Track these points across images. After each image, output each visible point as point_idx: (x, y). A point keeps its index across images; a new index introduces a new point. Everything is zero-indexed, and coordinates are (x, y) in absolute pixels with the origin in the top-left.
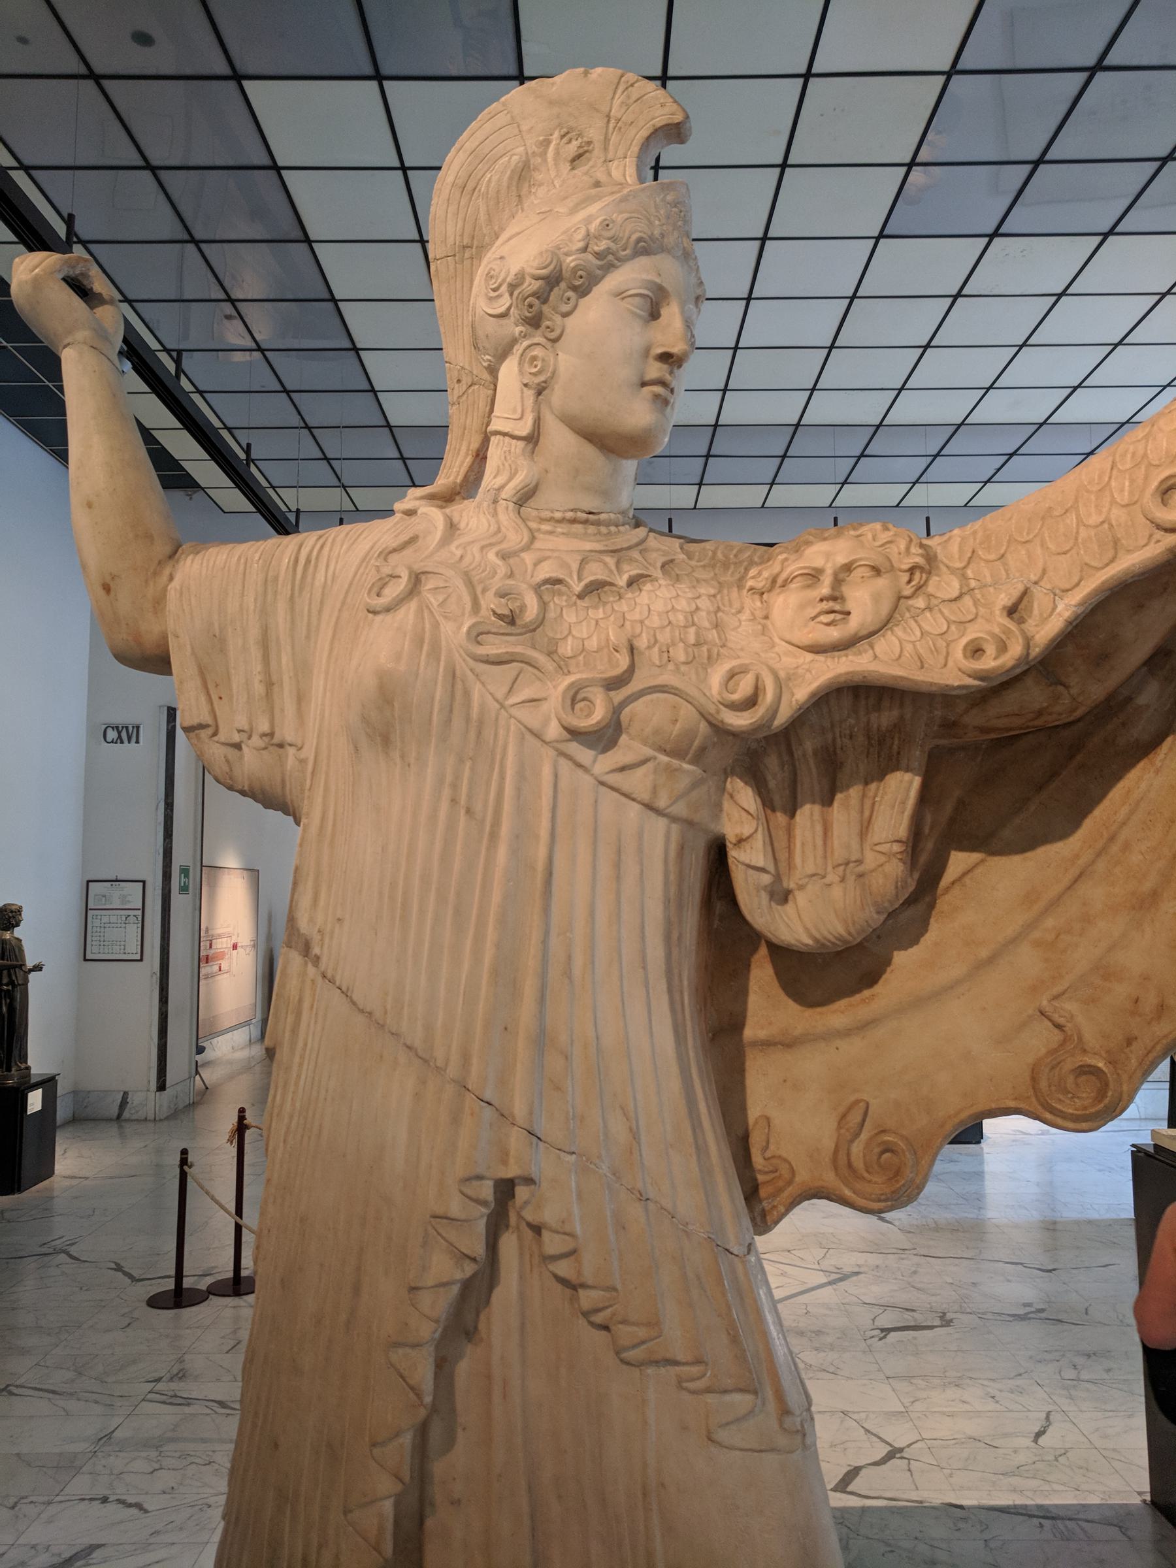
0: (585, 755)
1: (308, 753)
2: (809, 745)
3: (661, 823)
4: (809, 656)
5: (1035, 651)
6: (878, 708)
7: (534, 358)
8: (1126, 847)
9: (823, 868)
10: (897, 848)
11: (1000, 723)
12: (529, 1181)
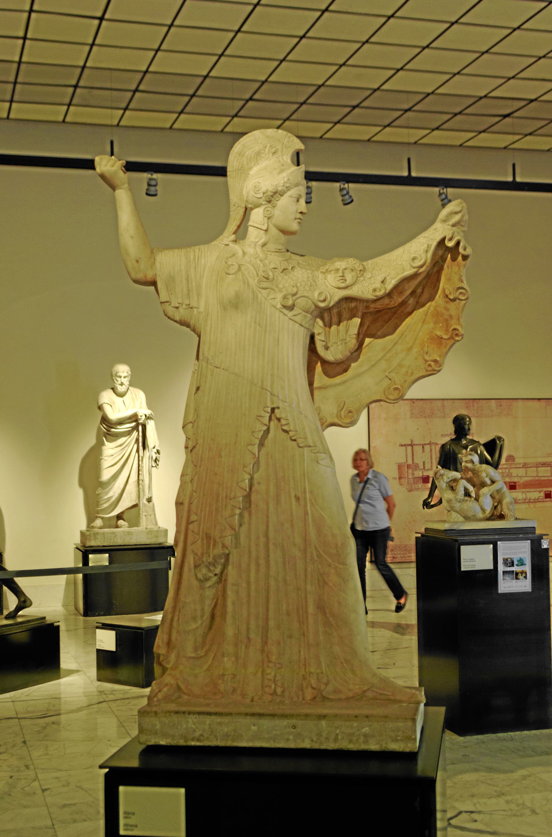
0: (286, 312)
1: (201, 309)
2: (335, 311)
3: (303, 329)
4: (337, 290)
5: (387, 291)
6: (351, 302)
7: (268, 210)
8: (406, 336)
10: (355, 336)
11: (378, 307)
12: (278, 408)
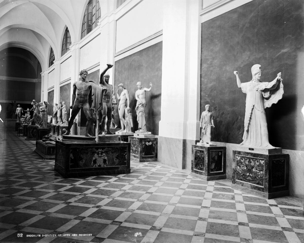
9: (267, 95)
